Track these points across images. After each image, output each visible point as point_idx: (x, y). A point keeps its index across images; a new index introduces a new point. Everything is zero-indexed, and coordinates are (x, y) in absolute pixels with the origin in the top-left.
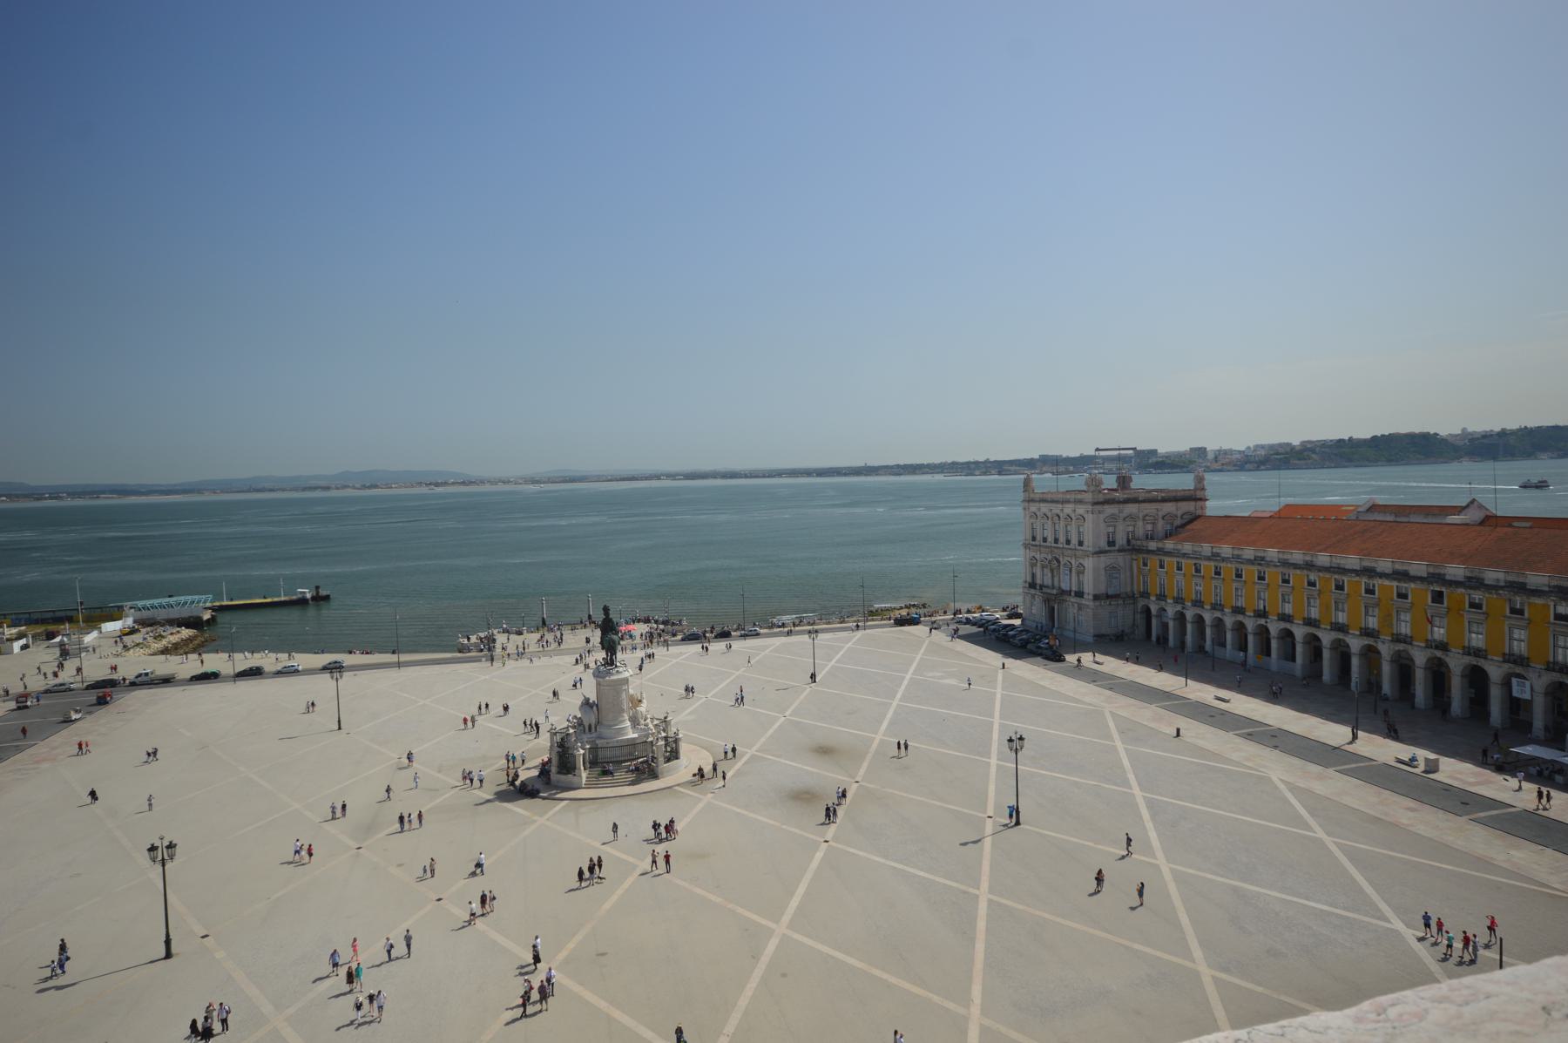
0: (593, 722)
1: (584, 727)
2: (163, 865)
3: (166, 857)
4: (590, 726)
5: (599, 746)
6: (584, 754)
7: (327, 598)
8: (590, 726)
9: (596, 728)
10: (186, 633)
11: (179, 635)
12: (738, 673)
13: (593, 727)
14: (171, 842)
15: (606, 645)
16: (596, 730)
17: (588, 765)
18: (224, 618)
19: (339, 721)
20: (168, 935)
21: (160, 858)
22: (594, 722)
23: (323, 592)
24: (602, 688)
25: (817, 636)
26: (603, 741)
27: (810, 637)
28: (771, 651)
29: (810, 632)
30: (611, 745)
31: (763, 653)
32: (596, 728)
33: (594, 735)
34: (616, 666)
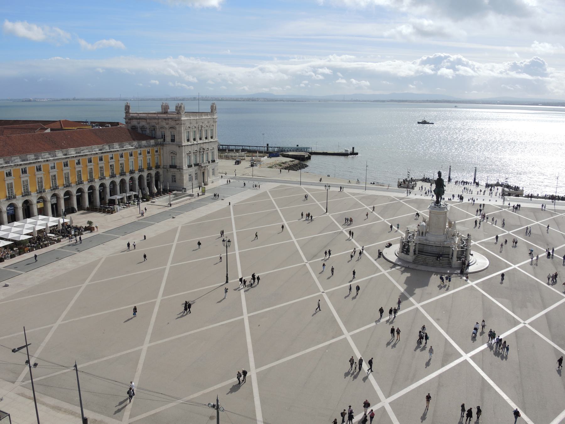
0: (424, 232)
1: (420, 232)
2: (227, 248)
3: (227, 245)
4: (422, 233)
6: (414, 246)
7: (357, 154)
8: (422, 233)
9: (425, 234)
10: (297, 162)
11: (293, 163)
12: (537, 223)
13: (424, 234)
14: (229, 240)
15: (436, 193)
17: (417, 252)
18: (313, 157)
19: (327, 209)
20: (227, 274)
21: (226, 245)
22: (425, 231)
23: (355, 151)
24: (431, 214)
30: (430, 244)
32: (425, 234)
33: (424, 238)
34: (440, 204)
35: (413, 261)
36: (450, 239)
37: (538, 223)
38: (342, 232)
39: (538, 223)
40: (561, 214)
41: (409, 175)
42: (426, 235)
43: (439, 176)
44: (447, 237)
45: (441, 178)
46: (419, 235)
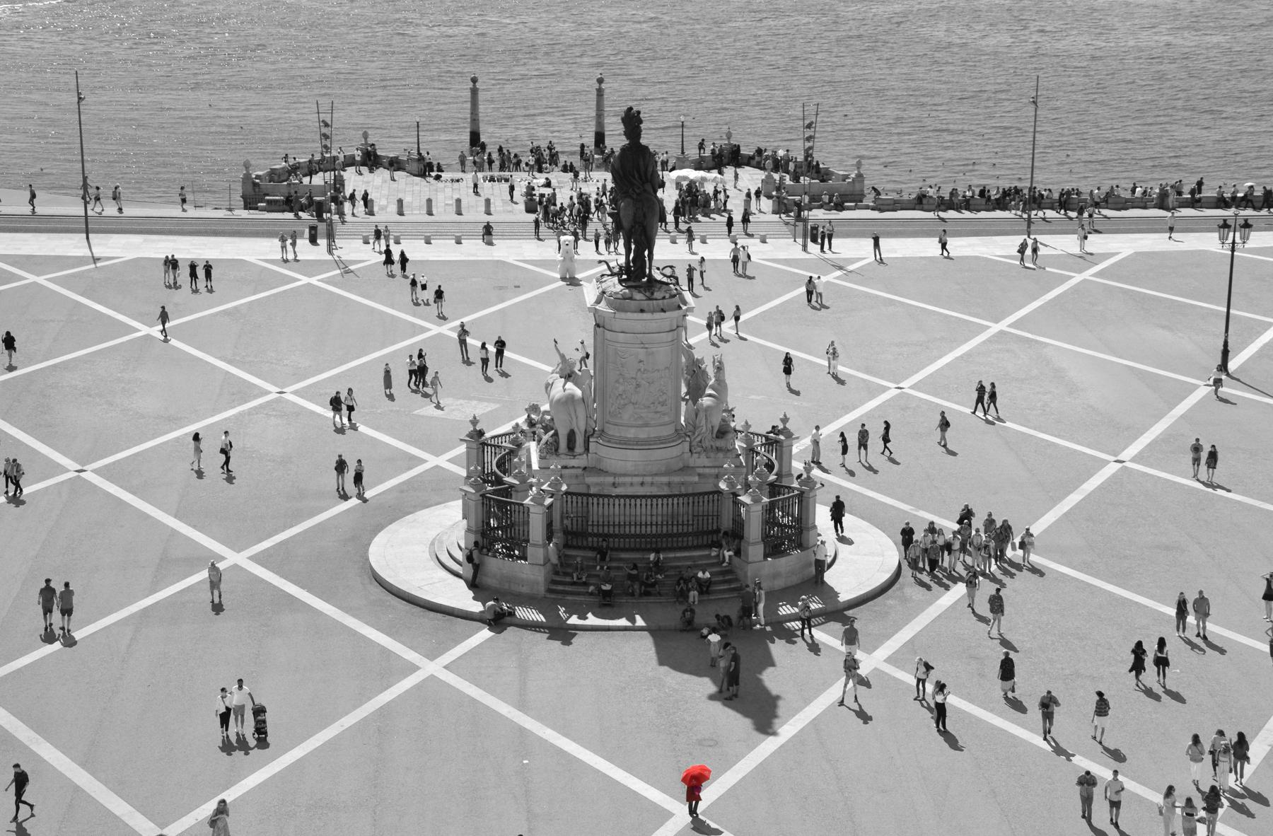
1: (556, 434)
4: (571, 436)
5: (593, 491)
12: (995, 328)
13: (580, 440)
16: (587, 449)
22: (583, 428)
24: (609, 335)
25: (1245, 239)
26: (600, 479)
27: (1223, 239)
28: (1100, 274)
29: (1225, 225)
31: (1078, 278)
35: (550, 591)
36: (712, 455)
37: (1003, 325)
38: (78, 485)
39: (1003, 325)
40: (1078, 278)
41: (326, 136)
42: (592, 446)
43: (626, 134)
44: (694, 443)
45: (643, 141)
46: (556, 450)
